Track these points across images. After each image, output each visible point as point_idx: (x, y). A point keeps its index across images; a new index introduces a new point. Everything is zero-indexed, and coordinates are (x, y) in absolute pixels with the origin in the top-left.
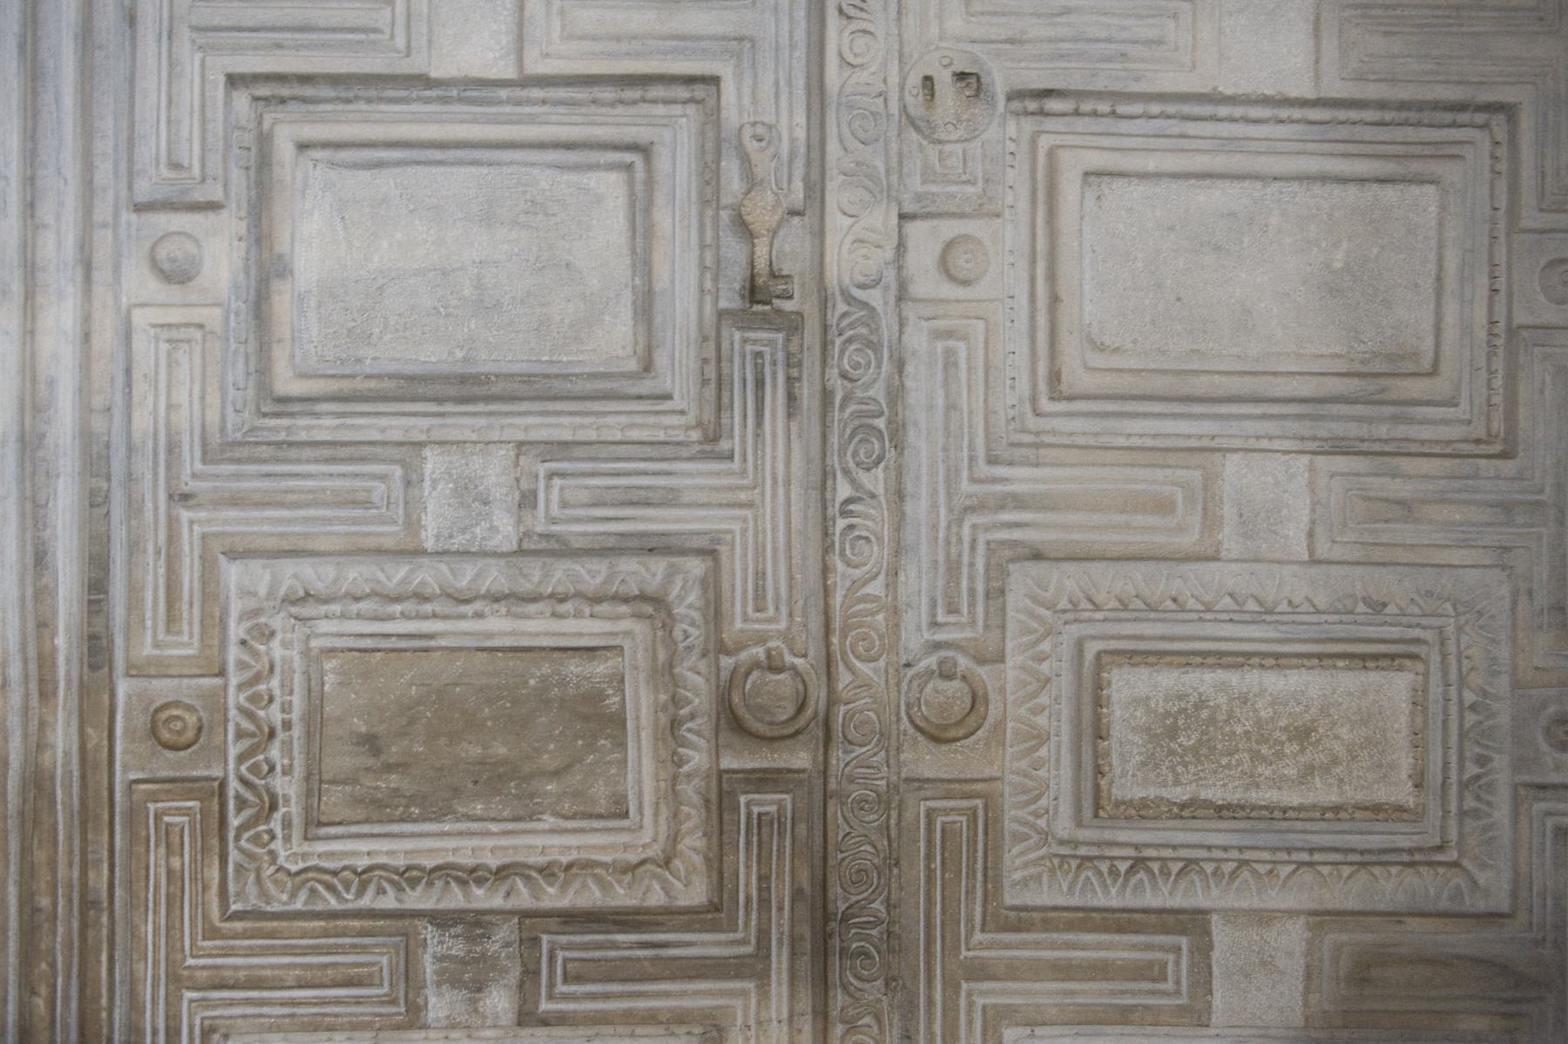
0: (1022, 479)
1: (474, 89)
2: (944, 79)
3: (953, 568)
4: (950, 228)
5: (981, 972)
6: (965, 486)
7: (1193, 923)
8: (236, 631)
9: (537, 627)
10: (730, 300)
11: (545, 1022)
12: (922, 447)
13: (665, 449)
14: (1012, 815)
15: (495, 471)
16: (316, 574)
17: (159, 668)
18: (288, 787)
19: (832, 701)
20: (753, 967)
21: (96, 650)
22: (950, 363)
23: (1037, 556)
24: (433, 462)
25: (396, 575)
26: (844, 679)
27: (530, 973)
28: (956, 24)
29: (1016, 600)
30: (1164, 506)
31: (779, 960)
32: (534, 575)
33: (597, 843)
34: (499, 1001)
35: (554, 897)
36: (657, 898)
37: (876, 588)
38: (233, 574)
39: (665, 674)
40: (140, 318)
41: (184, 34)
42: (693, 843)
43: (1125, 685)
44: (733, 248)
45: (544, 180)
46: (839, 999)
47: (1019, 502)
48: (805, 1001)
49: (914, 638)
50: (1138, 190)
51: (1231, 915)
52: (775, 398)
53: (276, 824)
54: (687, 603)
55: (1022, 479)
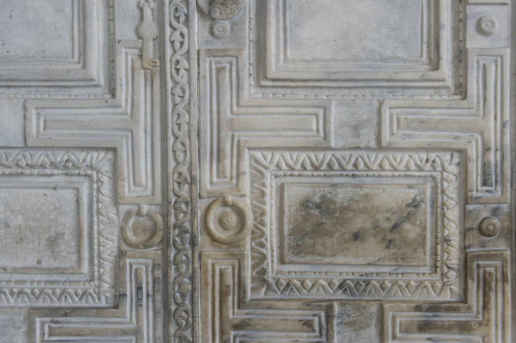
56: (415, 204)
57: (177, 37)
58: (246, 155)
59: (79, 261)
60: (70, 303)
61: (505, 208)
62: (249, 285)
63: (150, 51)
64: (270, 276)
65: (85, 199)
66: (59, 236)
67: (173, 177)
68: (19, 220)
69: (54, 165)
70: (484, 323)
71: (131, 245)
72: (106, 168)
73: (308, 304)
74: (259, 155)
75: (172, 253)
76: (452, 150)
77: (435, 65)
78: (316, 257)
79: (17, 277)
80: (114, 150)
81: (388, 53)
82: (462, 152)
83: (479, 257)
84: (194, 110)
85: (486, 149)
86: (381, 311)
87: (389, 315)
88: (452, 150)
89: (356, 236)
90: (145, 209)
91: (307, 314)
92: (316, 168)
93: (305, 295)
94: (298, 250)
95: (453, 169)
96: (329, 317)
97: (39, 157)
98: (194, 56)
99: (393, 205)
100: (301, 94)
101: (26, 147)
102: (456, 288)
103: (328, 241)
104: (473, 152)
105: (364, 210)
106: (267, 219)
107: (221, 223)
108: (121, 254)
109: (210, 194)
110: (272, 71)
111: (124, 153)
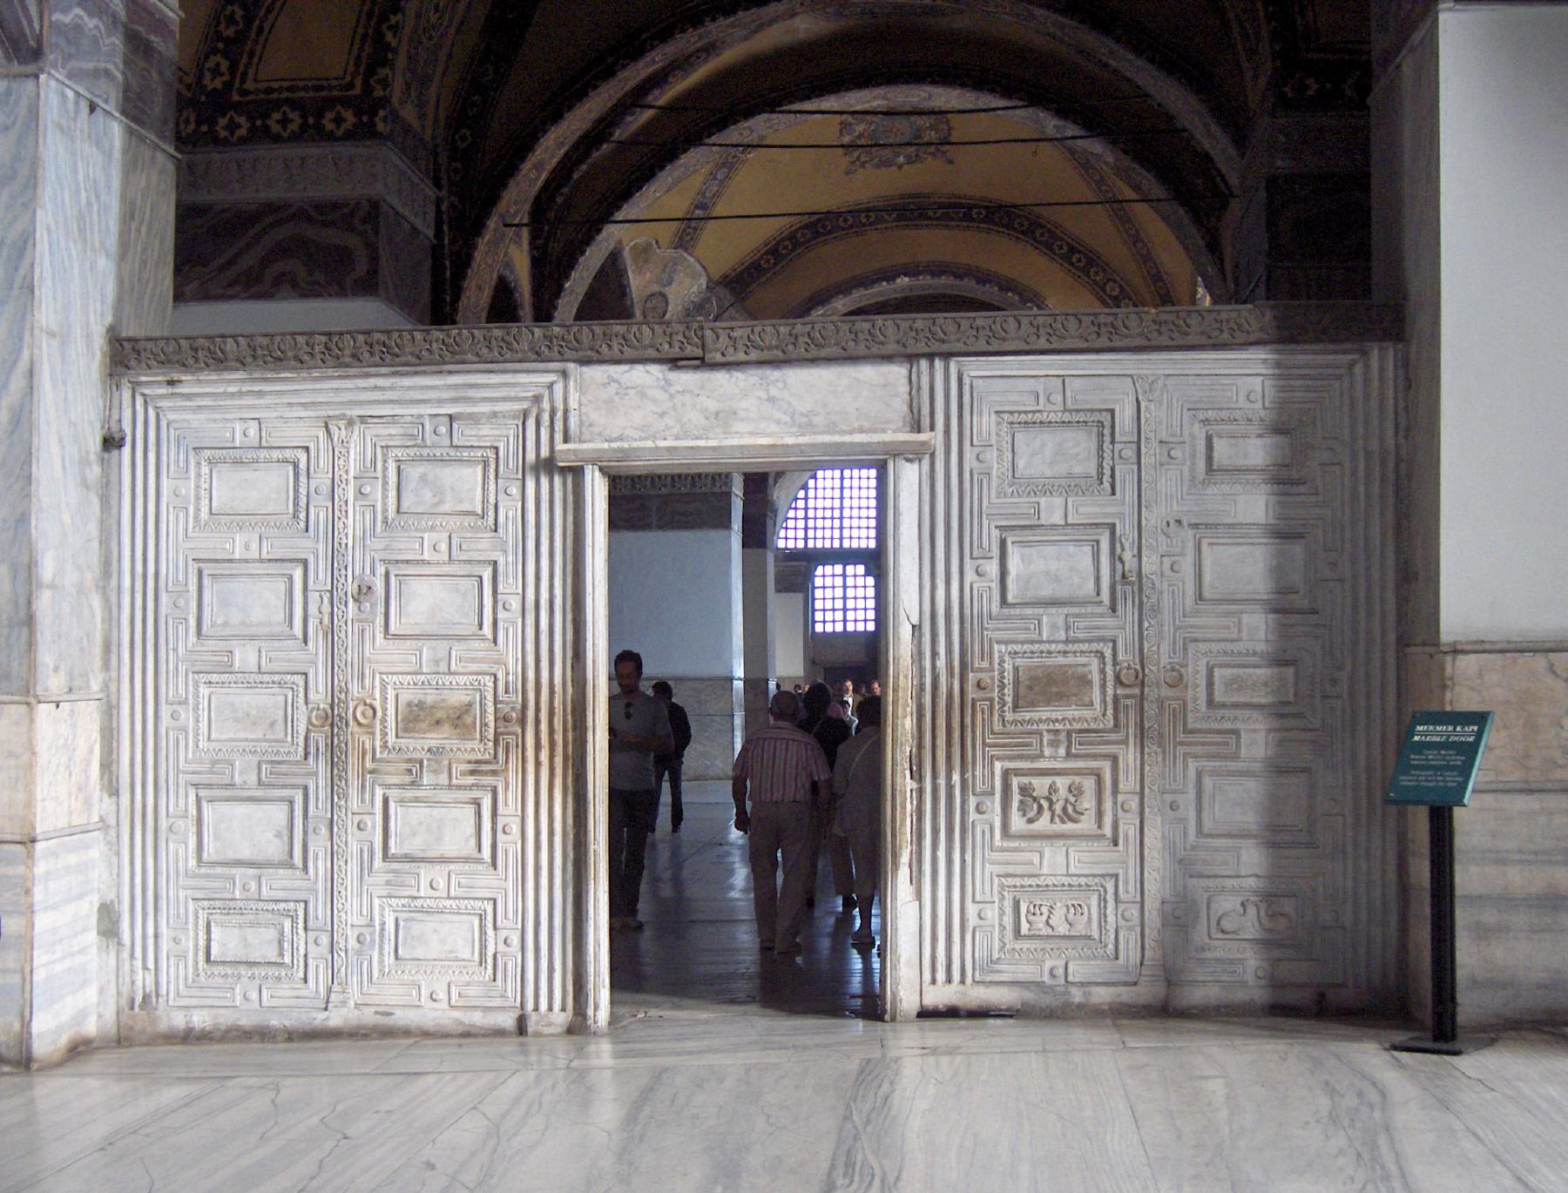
0: (1191, 621)
1: (1054, 526)
2: (1172, 522)
3: (1174, 643)
4: (1173, 559)
5: (1182, 744)
6: (1177, 623)
7: (1236, 732)
8: (997, 661)
9: (1070, 660)
10: (1118, 578)
11: (1077, 756)
12: (1166, 616)
13: (1102, 615)
14: (1190, 706)
15: (1061, 622)
16: (1017, 648)
17: (981, 670)
18: (1009, 699)
19: (1144, 675)
20: (1125, 742)
21: (964, 666)
22: (1173, 592)
23: (1196, 640)
24: (1045, 619)
25: (1036, 647)
26: (1147, 671)
27: (1070, 743)
28: (1175, 507)
29: (1190, 652)
30: (1228, 628)
31: (1131, 740)
32: (1070, 647)
33: (1087, 713)
34: (1062, 751)
35: (1077, 726)
36: (1102, 726)
37: (1155, 648)
38: (996, 647)
39: (1103, 671)
40: (975, 586)
41: (984, 517)
42: (1110, 712)
43: (1217, 673)
44: (1119, 566)
45: (1071, 549)
46: (1146, 749)
47: (1192, 627)
48: (1138, 750)
49: (1164, 660)
50: (1222, 547)
51: (1247, 731)
52: (1129, 602)
53: (1006, 708)
54: (1108, 653)
55: (1191, 621)
56: (470, 705)
57: (340, 613)
58: (377, 676)
59: (286, 734)
60: (281, 759)
61: (519, 706)
62: (378, 750)
63: (326, 620)
64: (390, 745)
65: (290, 701)
66: (275, 721)
67: (336, 689)
68: (254, 712)
69: (274, 682)
70: (507, 769)
71: (314, 726)
72: (302, 683)
73: (409, 760)
74: (384, 677)
75: (336, 730)
76: (491, 674)
77: (481, 626)
78: (416, 735)
79: (252, 744)
80: (306, 674)
81: (456, 620)
82: (495, 676)
83: (503, 734)
84: (349, 651)
85: (507, 674)
86: (450, 764)
87: (454, 766)
88: (491, 674)
89: (438, 722)
90: (322, 706)
91: (409, 766)
92: (415, 684)
93: (409, 756)
94: (406, 730)
95: (491, 685)
96: (421, 767)
97: (266, 678)
98: (349, 623)
99: (457, 704)
100: (408, 643)
101: (260, 673)
102: (492, 752)
103: (424, 726)
104: (500, 675)
105: (442, 708)
106: (389, 713)
107: (363, 714)
108: (308, 731)
109: (358, 698)
110: (392, 629)
111: (311, 677)
